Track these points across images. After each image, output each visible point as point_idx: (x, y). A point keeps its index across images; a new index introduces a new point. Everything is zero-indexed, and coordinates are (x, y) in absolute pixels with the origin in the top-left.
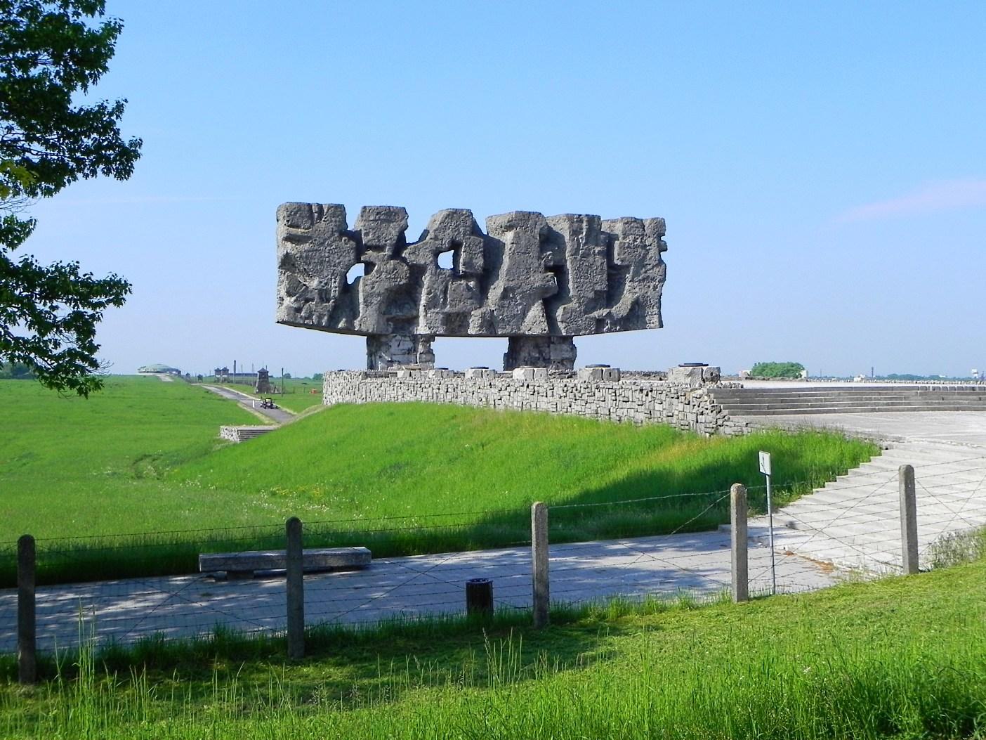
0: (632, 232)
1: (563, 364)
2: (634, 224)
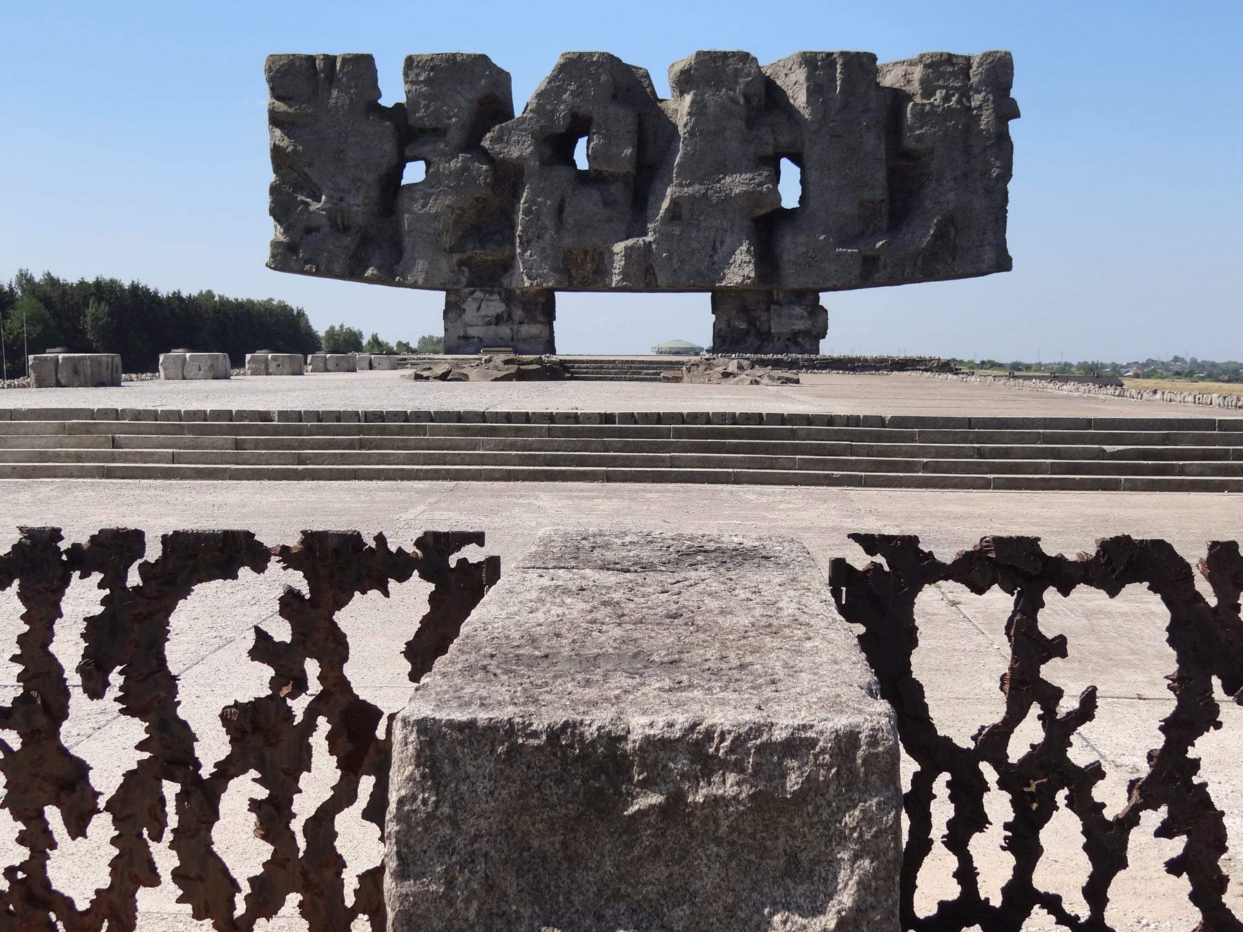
0: (941, 82)
1: (797, 343)
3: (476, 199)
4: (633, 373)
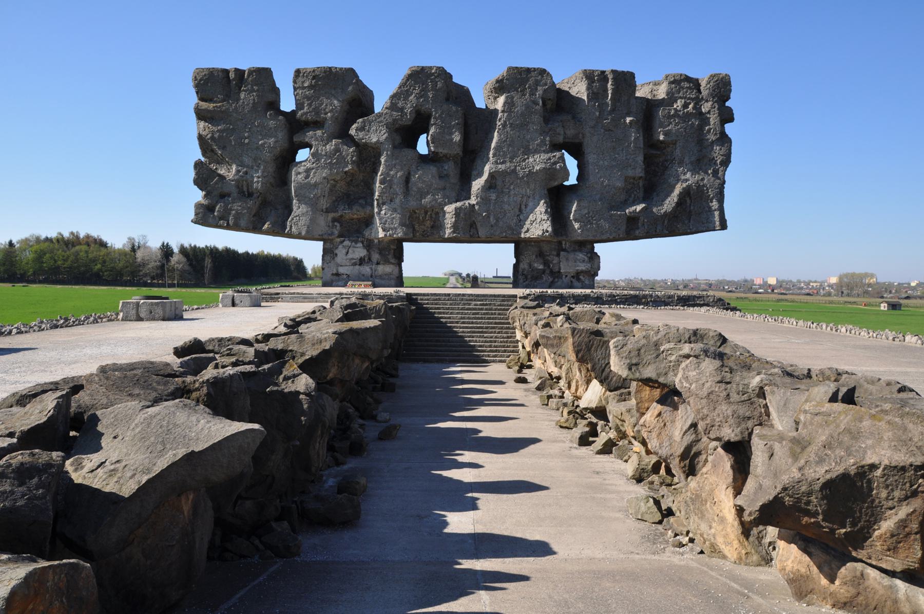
0: (681, 94)
1: (579, 280)
2: (686, 85)
3: (346, 172)
4: (464, 304)
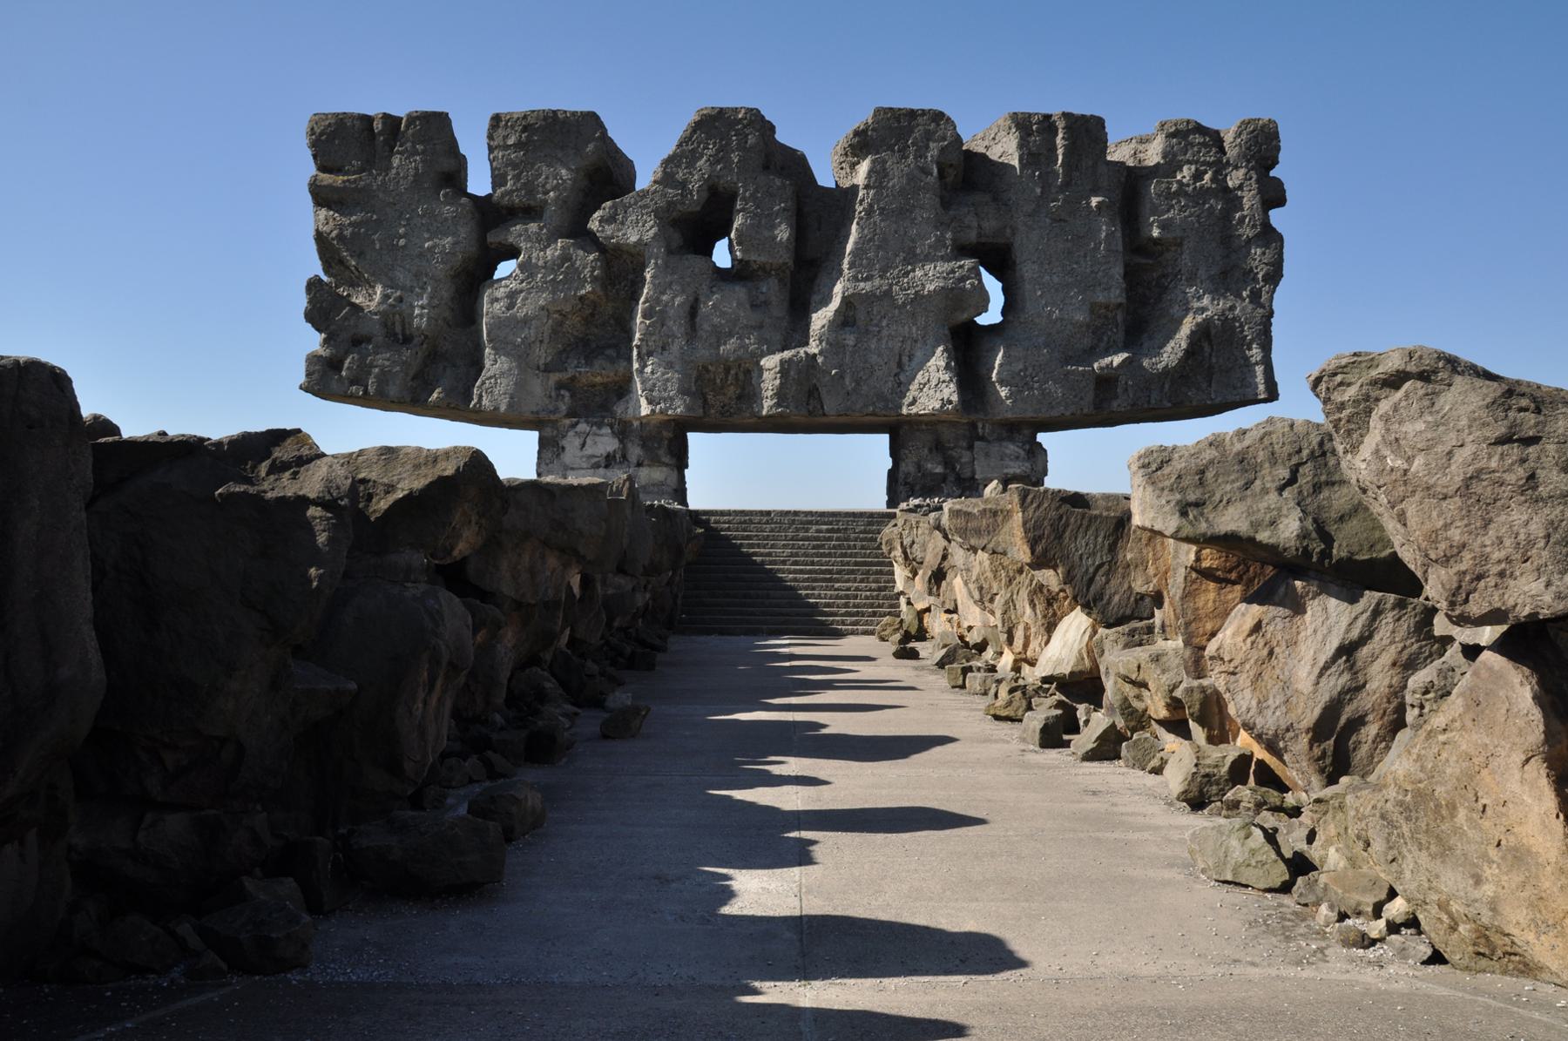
2: (1198, 139)
3: (581, 298)
